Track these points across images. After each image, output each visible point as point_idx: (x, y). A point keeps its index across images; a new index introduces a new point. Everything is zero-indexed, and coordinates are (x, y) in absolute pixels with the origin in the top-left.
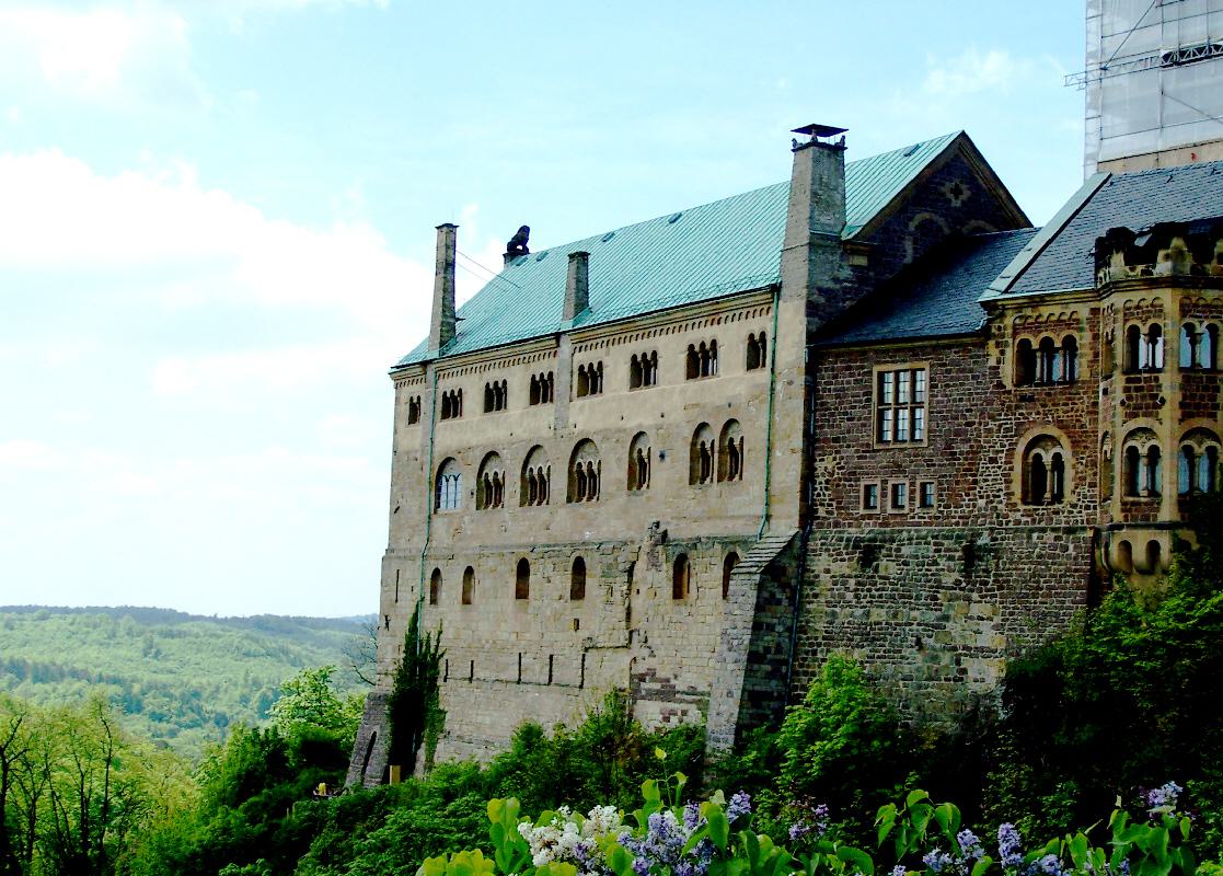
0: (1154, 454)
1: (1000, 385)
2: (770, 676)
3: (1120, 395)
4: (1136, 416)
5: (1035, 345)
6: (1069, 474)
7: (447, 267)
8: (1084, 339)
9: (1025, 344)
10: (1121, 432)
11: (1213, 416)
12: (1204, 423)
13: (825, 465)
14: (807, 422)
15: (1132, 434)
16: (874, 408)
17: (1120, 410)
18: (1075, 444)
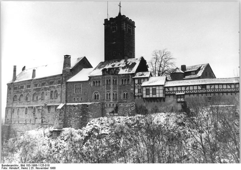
0: (110, 94)
1: (91, 86)
2: (62, 121)
3: (105, 88)
4: (107, 90)
5: (95, 82)
6: (99, 97)
7: (15, 71)
8: (101, 81)
9: (94, 82)
10: (106, 91)
11: (116, 90)
12: (116, 91)
13: (69, 96)
14: (66, 91)
15: (107, 92)
16: (75, 89)
17: (105, 89)
18: (100, 93)
